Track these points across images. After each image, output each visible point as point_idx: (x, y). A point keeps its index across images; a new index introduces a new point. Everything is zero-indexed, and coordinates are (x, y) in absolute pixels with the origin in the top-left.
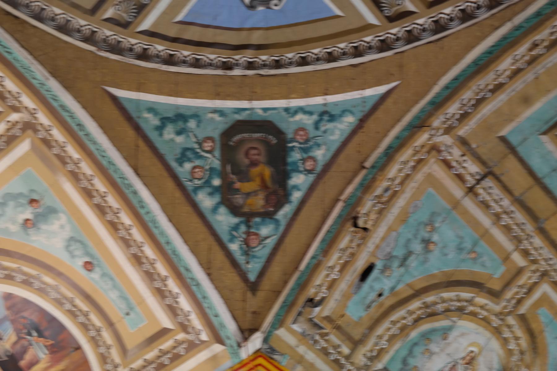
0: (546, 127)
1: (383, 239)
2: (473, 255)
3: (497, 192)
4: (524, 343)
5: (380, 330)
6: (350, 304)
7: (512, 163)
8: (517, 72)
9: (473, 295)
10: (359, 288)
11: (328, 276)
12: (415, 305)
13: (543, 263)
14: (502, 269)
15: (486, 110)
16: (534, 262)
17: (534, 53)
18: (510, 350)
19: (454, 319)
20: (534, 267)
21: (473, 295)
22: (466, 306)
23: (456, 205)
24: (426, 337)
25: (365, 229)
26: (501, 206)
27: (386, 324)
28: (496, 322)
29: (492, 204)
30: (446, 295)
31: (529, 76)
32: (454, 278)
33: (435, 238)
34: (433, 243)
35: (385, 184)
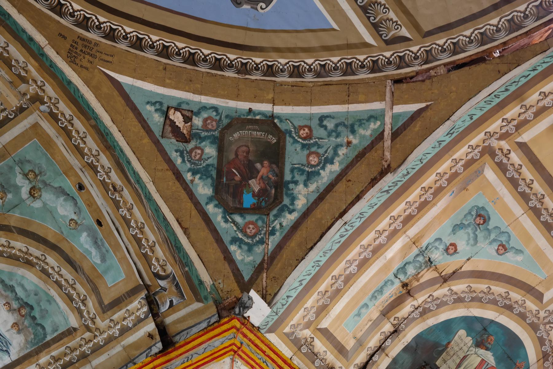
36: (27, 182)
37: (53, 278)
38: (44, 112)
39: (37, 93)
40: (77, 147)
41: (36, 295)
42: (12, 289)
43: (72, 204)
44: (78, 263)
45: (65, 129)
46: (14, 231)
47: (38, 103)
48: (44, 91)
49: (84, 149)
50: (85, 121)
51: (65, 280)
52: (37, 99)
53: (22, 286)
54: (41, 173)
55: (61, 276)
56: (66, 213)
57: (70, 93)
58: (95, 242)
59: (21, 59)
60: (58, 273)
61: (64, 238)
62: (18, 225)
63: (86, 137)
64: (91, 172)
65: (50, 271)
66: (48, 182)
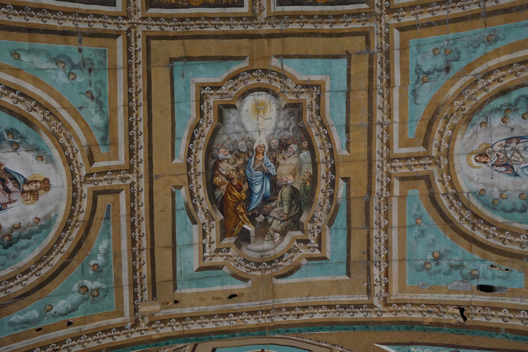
0: (324, 262)
1: (458, 292)
2: (419, 221)
3: (375, 246)
4: (439, 125)
5: (516, 248)
6: (516, 287)
7: (355, 255)
8: (316, 307)
9: (441, 197)
10: (500, 288)
11: (511, 318)
12: (479, 235)
13: (385, 170)
14: (410, 192)
15: (345, 299)
16: (389, 175)
17: (302, 312)
18: (453, 131)
19: (465, 195)
20: (393, 171)
21: (440, 195)
22: (452, 195)
23: (402, 261)
24: (493, 206)
25: (462, 310)
26: (379, 233)
27: (508, 246)
28: (444, 162)
29: (383, 241)
30: (457, 218)
31: (312, 300)
32: (443, 221)
33: (430, 257)
34: (433, 256)
35: (428, 316)
36: (93, 288)
37: (19, 276)
38: (127, 324)
39: (139, 327)
40: (95, 334)
41: (14, 257)
42: (28, 237)
43: (62, 312)
44: (20, 301)
45: (110, 330)
46: (68, 260)
47: (134, 323)
48: (138, 331)
49: (92, 338)
50: (107, 346)
51: (13, 286)
52: (136, 324)
53: (25, 247)
54: (93, 300)
55: (17, 284)
56: (59, 305)
57: (128, 347)
58: (28, 322)
59: (162, 331)
60: (21, 282)
61: (43, 297)
62: (69, 266)
63: (98, 342)
64: (75, 335)
65: (25, 277)
66: (85, 302)
